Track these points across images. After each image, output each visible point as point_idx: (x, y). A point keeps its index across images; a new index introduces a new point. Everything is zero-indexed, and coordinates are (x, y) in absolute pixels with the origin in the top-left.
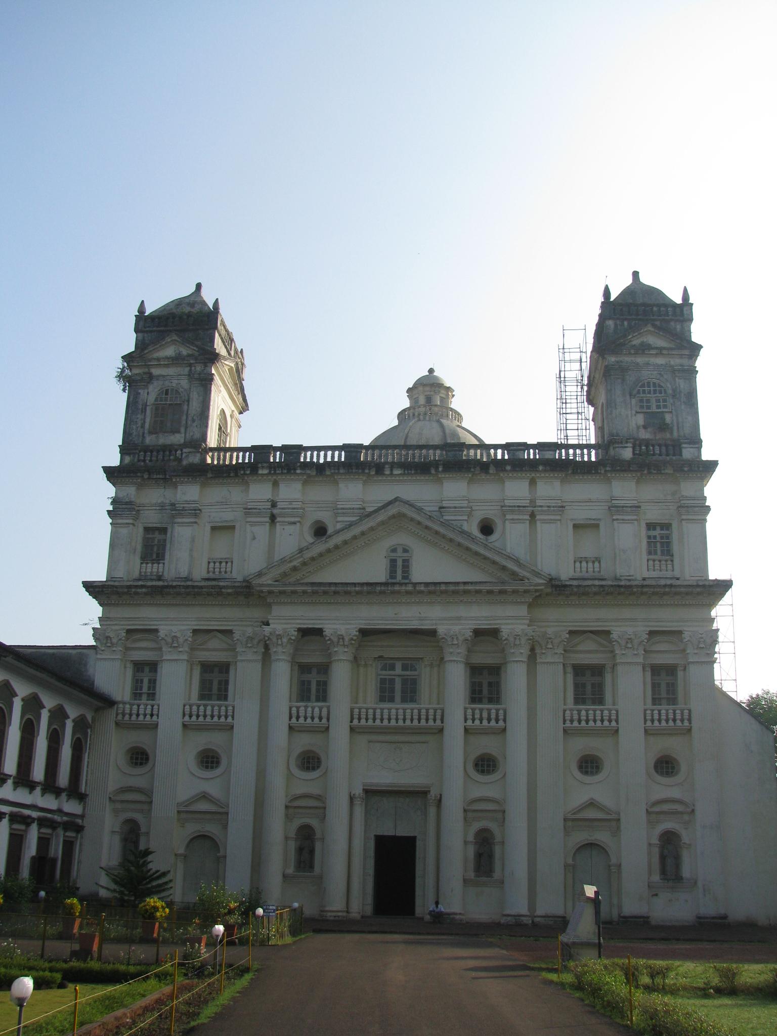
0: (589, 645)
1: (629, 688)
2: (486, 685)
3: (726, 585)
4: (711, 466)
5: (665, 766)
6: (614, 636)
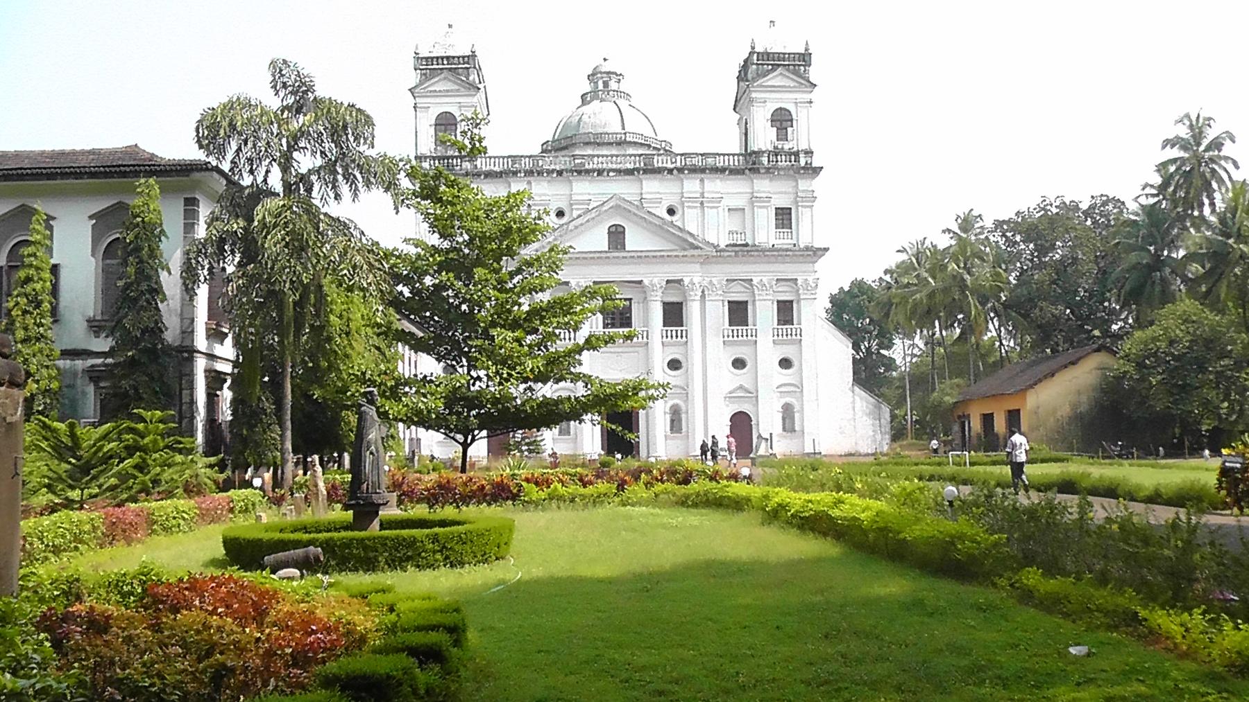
0: (736, 287)
1: (764, 314)
2: (674, 315)
3: (826, 250)
4: (817, 171)
5: (785, 363)
6: (755, 282)
